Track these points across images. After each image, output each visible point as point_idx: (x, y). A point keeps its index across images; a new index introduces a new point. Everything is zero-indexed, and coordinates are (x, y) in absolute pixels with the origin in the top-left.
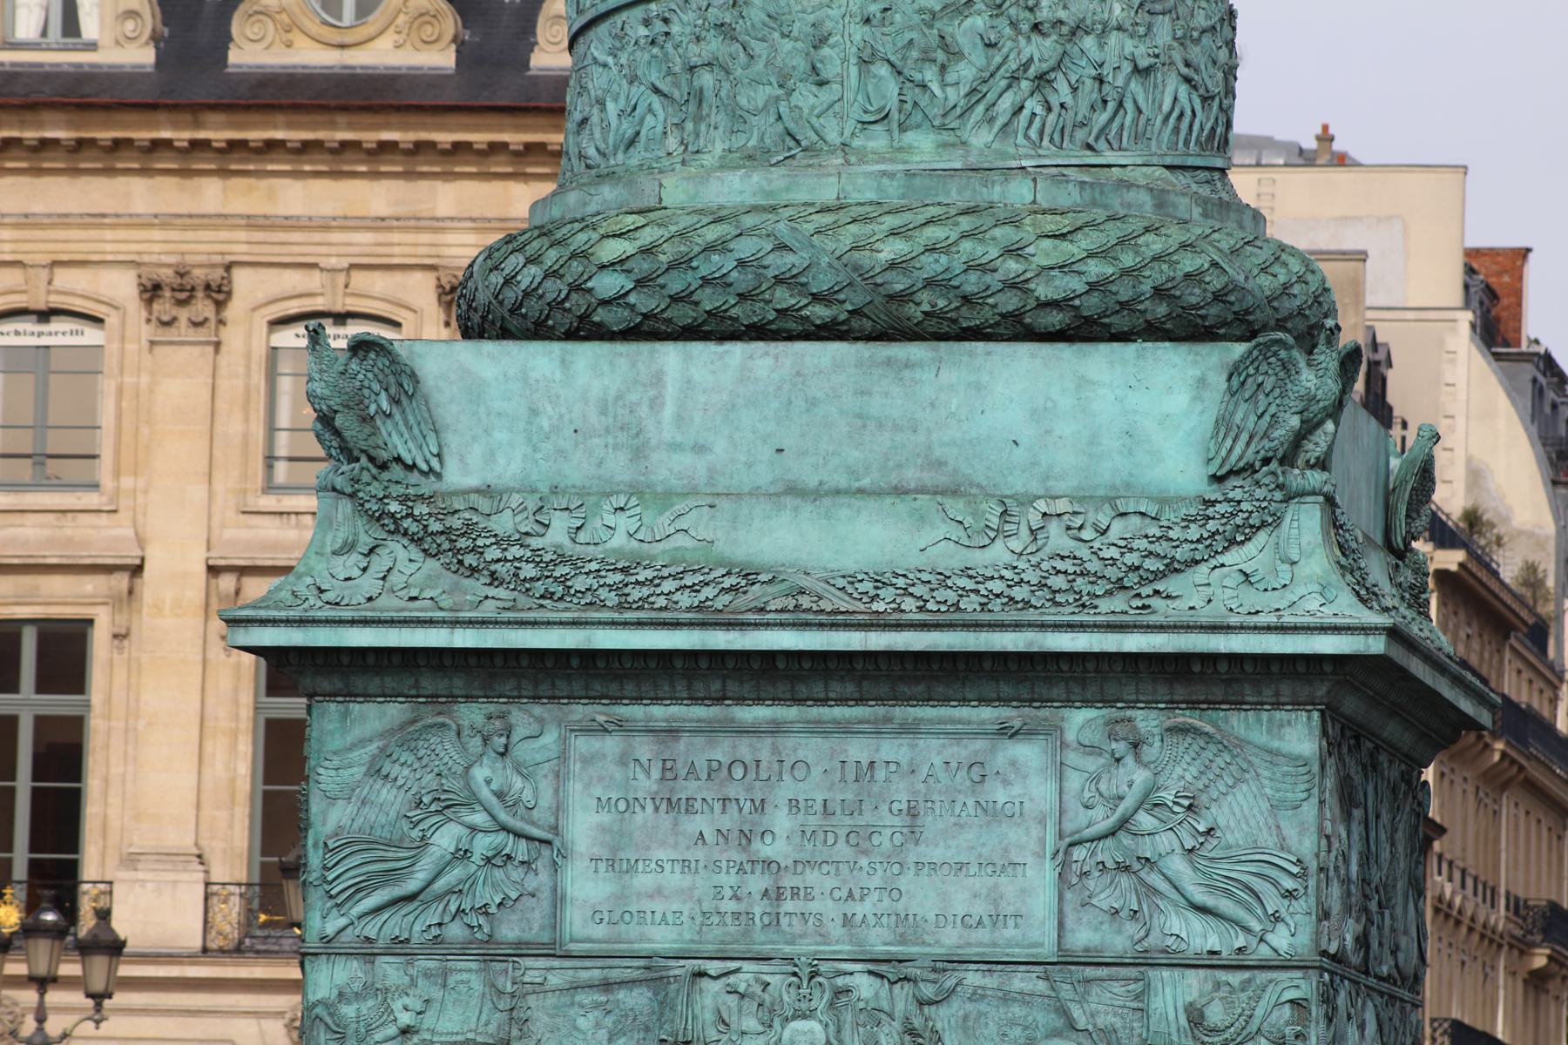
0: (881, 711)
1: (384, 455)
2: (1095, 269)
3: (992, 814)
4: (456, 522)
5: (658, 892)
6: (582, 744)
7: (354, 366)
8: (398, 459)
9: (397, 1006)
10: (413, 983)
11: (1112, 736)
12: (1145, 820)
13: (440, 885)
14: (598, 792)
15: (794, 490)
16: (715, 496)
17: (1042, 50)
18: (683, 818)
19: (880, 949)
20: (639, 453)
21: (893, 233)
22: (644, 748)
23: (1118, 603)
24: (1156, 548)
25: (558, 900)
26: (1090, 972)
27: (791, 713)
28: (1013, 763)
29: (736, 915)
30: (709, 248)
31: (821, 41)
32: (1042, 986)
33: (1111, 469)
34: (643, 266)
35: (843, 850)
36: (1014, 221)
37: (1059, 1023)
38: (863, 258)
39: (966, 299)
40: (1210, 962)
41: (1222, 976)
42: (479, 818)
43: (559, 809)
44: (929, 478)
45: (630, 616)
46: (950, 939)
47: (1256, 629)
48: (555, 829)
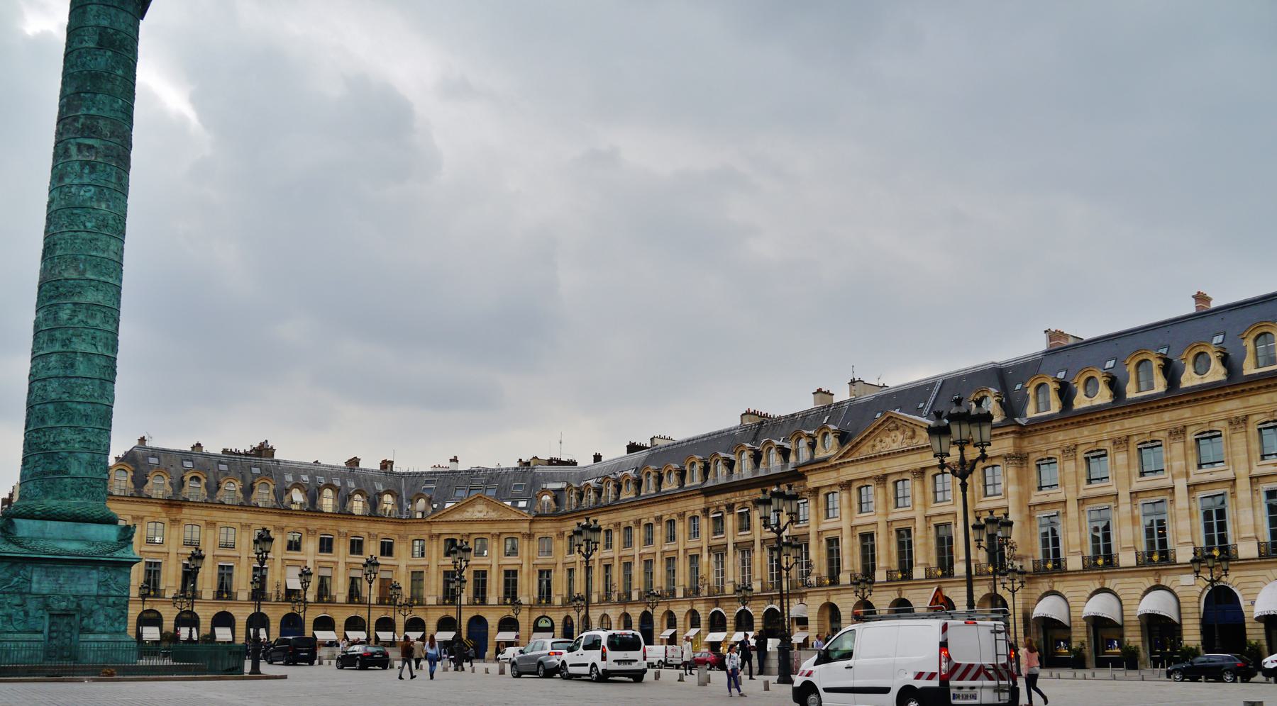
33: (106, 538)
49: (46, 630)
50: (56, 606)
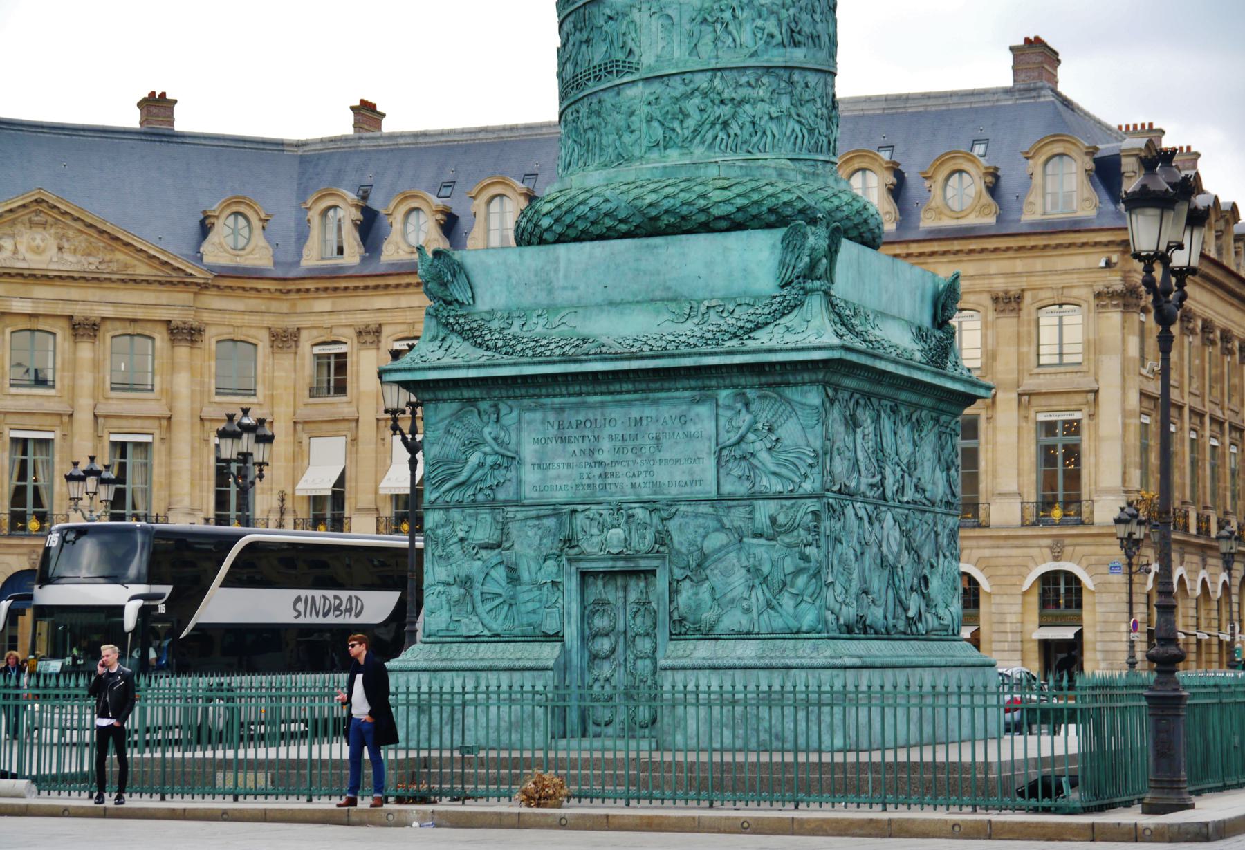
0: (644, 395)
1: (449, 299)
2: (740, 202)
3: (689, 436)
4: (474, 325)
5: (558, 477)
6: (528, 416)
7: (436, 262)
8: (457, 301)
9: (458, 529)
10: (465, 519)
11: (735, 401)
12: (751, 437)
13: (474, 478)
14: (534, 435)
15: (611, 303)
16: (578, 307)
17: (726, 111)
18: (568, 445)
19: (646, 497)
20: (550, 292)
21: (651, 191)
22: (551, 416)
23: (735, 343)
24: (751, 318)
25: (520, 482)
26: (730, 503)
27: (609, 398)
28: (698, 415)
29: (589, 485)
30: (580, 204)
31: (632, 114)
32: (711, 510)
34: (557, 213)
35: (630, 456)
36: (705, 184)
37: (718, 526)
38: (639, 203)
39: (683, 218)
40: (779, 496)
41: (784, 502)
42: (487, 449)
43: (519, 444)
44: (665, 295)
45: (535, 359)
46: (674, 492)
47: (787, 350)
48: (517, 452)
49: (572, 633)
50: (590, 545)
